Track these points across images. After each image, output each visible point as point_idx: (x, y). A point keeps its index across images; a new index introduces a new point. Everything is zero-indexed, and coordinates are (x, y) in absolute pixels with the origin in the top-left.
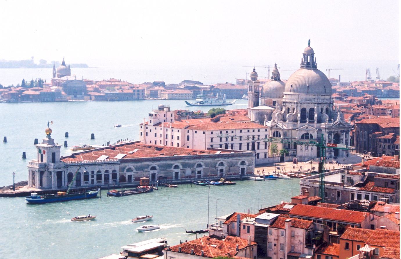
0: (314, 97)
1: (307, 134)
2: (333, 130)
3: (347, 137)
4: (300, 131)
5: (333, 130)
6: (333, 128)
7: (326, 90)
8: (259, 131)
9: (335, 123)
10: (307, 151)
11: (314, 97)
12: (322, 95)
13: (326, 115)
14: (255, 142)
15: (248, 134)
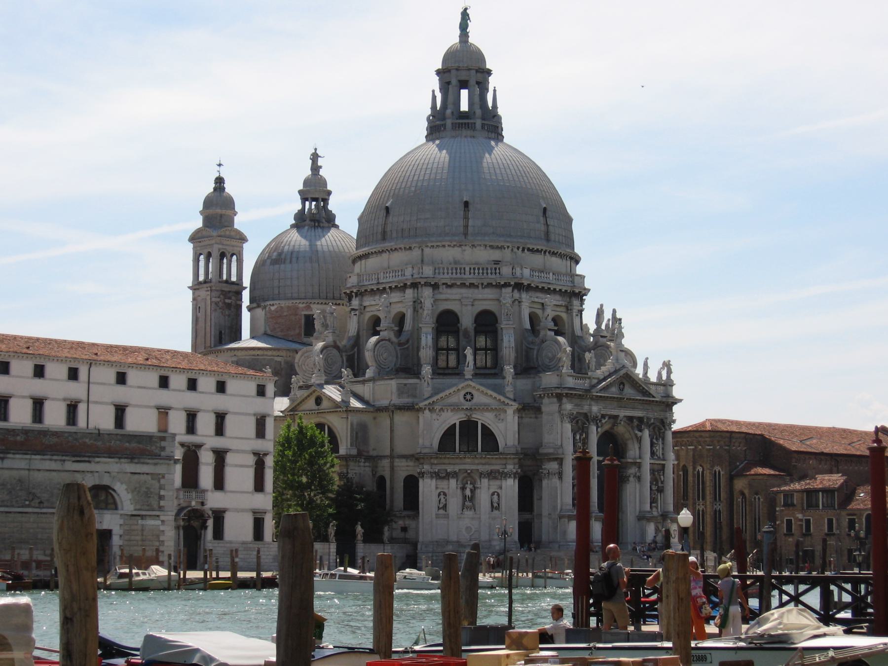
0: (496, 255)
1: (469, 427)
2: (595, 409)
3: (659, 453)
4: (431, 410)
5: (595, 409)
6: (592, 399)
7: (551, 228)
8: (221, 387)
9: (599, 373)
10: (469, 513)
11: (496, 255)
12: (531, 250)
13: (557, 342)
14: (199, 446)
15: (164, 397)
